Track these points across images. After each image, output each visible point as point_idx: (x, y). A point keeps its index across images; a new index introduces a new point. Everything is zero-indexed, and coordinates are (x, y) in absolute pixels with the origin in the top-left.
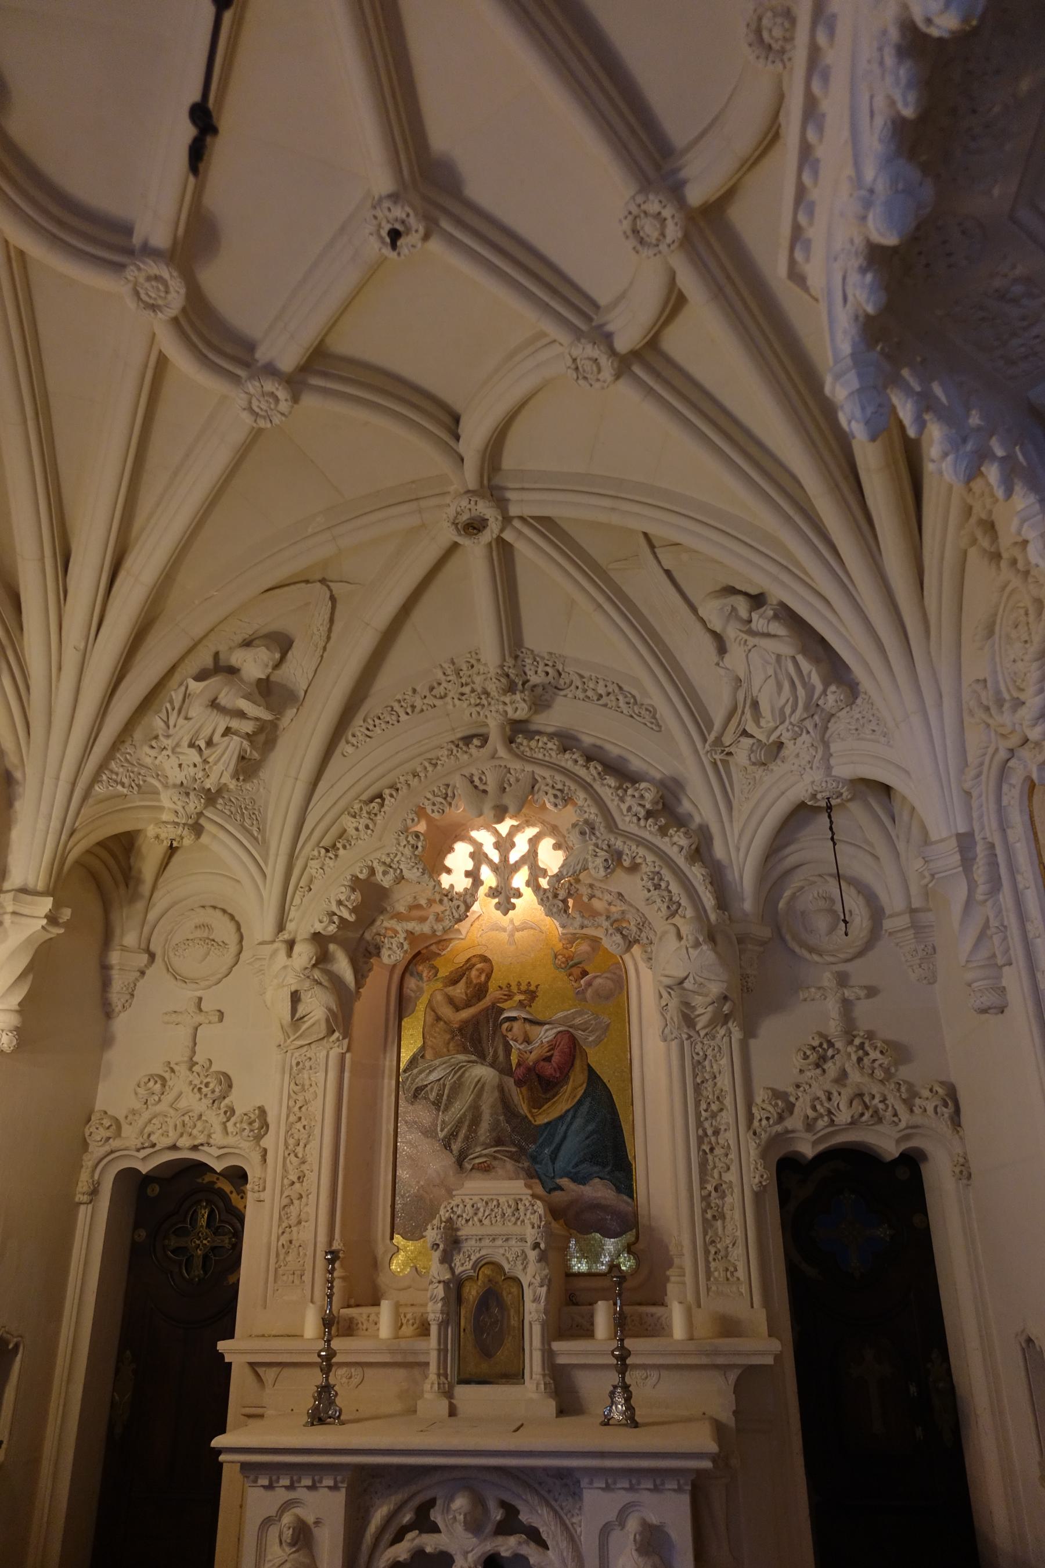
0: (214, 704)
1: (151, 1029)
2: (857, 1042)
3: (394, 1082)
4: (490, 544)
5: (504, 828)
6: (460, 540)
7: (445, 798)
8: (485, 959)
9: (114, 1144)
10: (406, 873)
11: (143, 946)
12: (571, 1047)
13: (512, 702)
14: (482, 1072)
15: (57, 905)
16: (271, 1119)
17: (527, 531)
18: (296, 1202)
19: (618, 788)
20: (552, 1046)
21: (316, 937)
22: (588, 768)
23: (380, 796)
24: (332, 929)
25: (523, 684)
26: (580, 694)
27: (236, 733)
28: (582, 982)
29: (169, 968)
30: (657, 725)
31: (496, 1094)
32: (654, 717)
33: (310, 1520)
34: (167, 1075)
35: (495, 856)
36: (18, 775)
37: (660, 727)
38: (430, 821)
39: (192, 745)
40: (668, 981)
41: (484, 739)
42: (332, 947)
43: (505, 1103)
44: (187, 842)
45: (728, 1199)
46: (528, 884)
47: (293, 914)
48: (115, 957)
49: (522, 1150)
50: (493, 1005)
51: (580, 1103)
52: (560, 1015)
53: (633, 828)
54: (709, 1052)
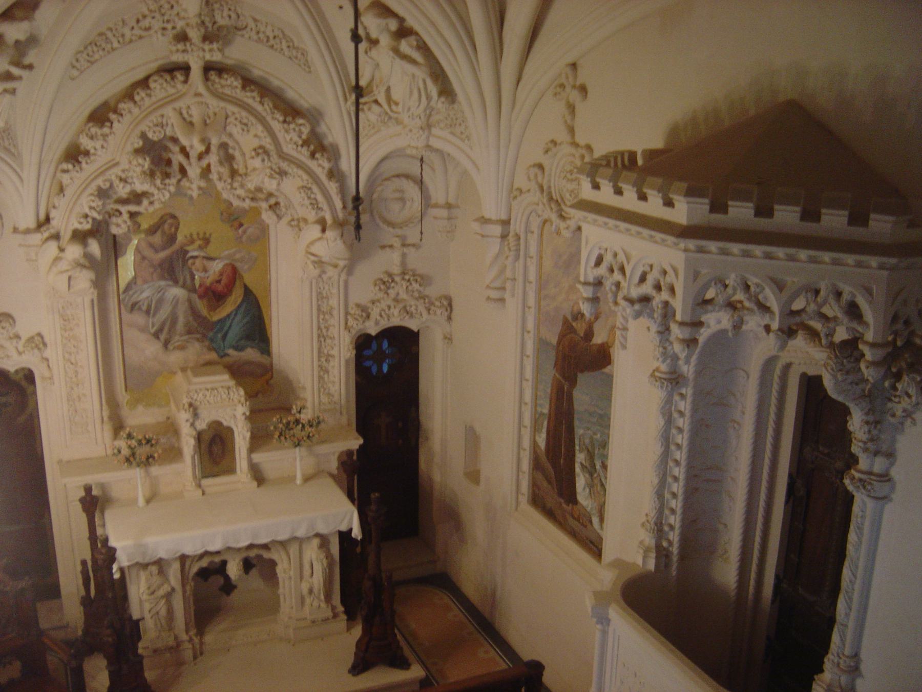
2: (407, 277)
7: (162, 127)
8: (174, 217)
12: (233, 274)
13: (211, 50)
14: (177, 292)
16: (47, 339)
18: (75, 389)
20: (221, 274)
22: (263, 105)
28: (240, 231)
30: (307, 67)
31: (187, 304)
37: (309, 67)
45: (332, 363)
49: (204, 336)
50: (182, 248)
51: (239, 307)
52: (227, 253)
53: (294, 153)
54: (327, 288)
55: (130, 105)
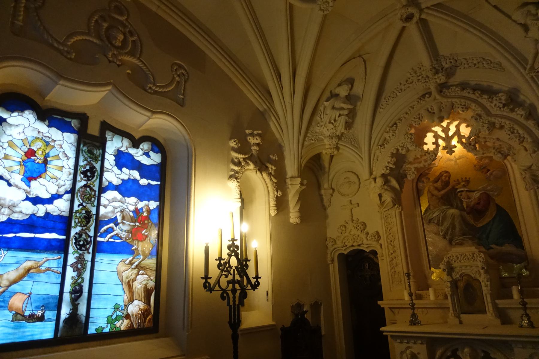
0: (333, 108)
1: (338, 212)
3: (421, 218)
4: (417, 22)
5: (444, 124)
6: (405, 25)
8: (447, 172)
9: (335, 246)
10: (409, 148)
11: (330, 187)
12: (487, 199)
14: (452, 211)
15: (302, 180)
16: (381, 234)
17: (431, 12)
19: (489, 99)
20: (479, 199)
21: (383, 175)
23: (395, 124)
24: (388, 171)
25: (442, 69)
26: (466, 66)
27: (343, 115)
29: (339, 193)
32: (501, 66)
33: (416, 352)
34: (346, 225)
35: (443, 135)
36: (283, 144)
38: (415, 128)
39: (330, 123)
40: (523, 168)
41: (430, 94)
42: (389, 177)
43: (464, 220)
44: (335, 153)
46: (458, 142)
47: (374, 169)
48: (323, 192)
50: (453, 188)
51: (495, 218)
52: (480, 188)
53: (499, 112)
55: (405, 115)
